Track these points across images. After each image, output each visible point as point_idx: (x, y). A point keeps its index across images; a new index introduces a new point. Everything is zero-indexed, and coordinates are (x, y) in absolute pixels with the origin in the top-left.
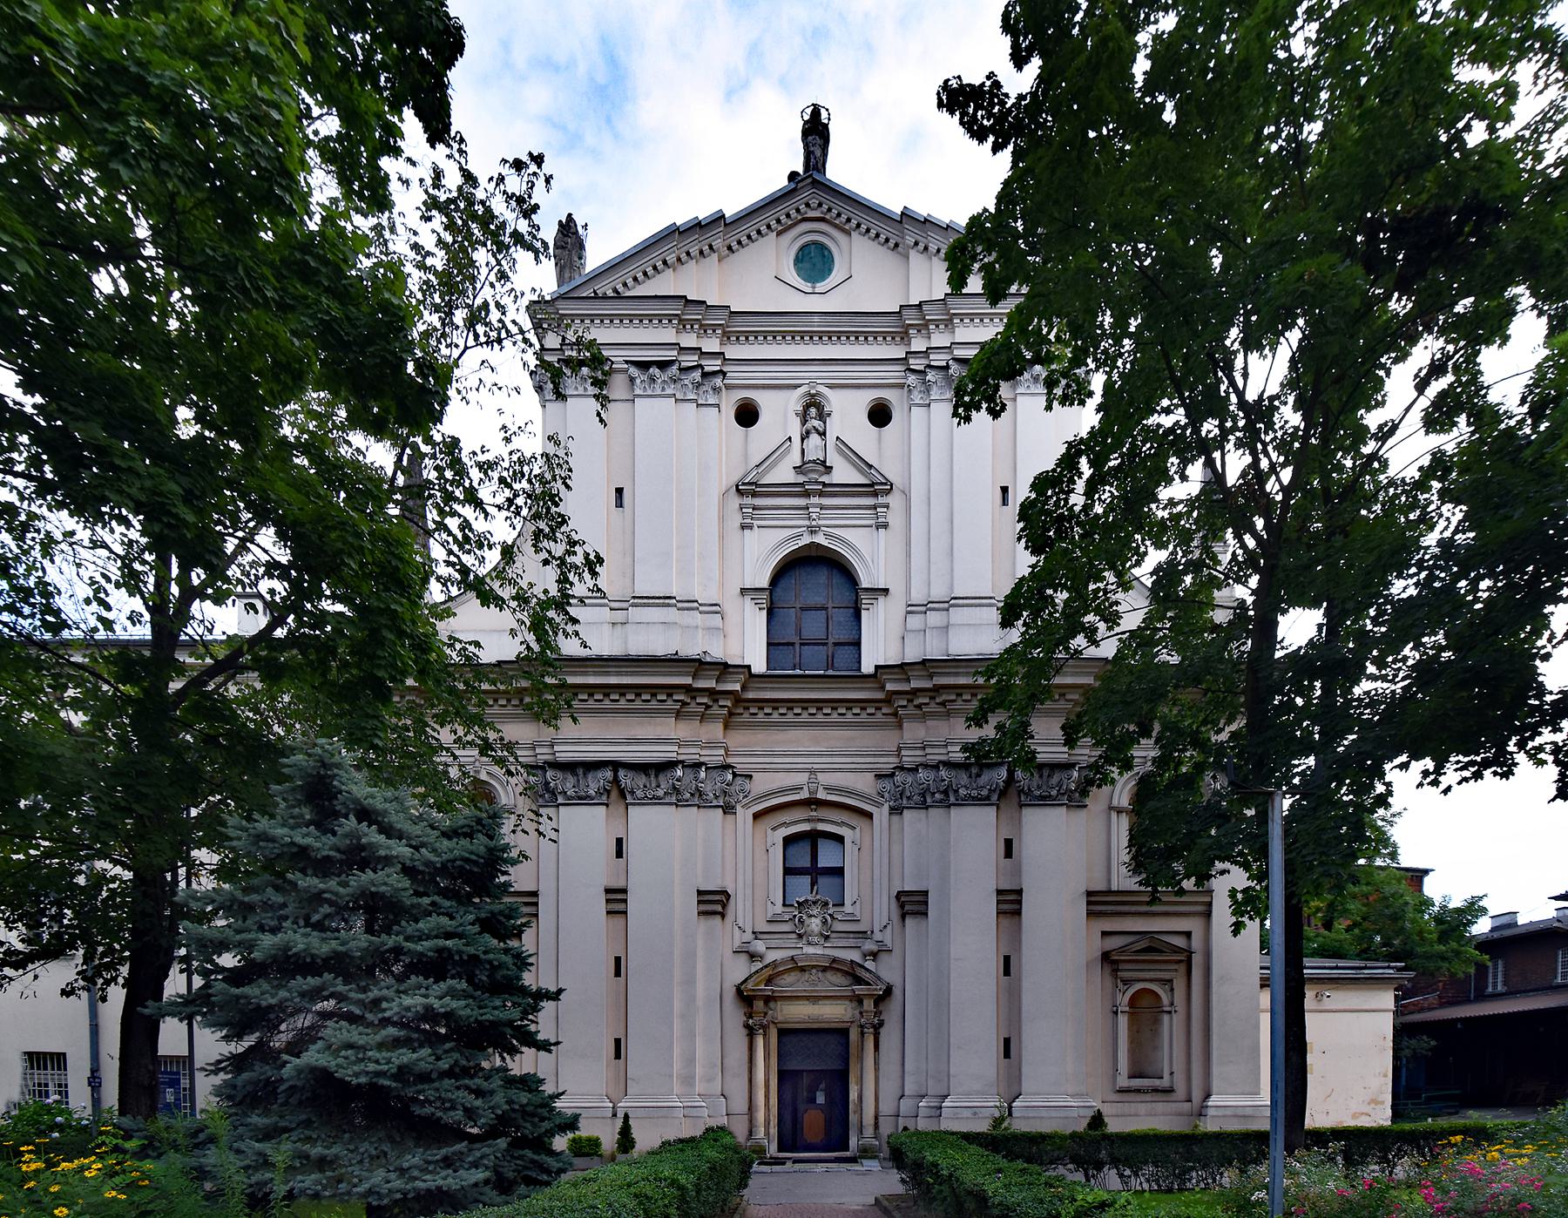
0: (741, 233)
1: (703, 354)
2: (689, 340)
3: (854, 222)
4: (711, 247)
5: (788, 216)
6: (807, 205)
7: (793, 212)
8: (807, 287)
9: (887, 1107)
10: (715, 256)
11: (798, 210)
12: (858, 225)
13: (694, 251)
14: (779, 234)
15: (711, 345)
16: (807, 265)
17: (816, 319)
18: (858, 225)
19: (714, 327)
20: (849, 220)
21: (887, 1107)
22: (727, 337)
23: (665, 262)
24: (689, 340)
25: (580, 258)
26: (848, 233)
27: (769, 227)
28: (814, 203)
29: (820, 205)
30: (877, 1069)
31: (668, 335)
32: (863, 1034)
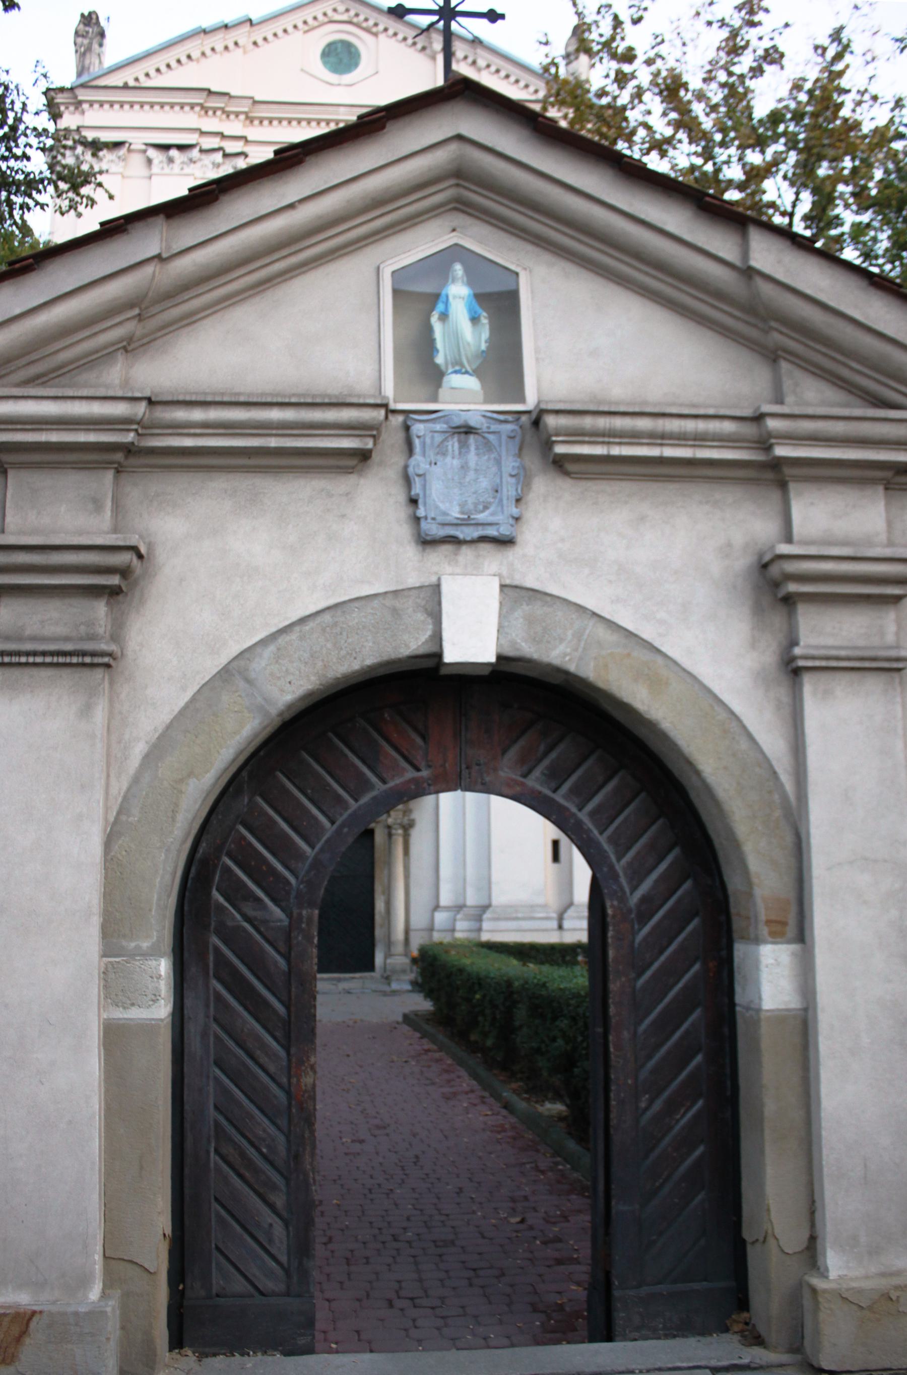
0: (267, 30)
1: (223, 136)
2: (211, 124)
3: (381, 27)
4: (236, 44)
5: (315, 18)
6: (335, 10)
7: (321, 18)
8: (333, 78)
9: (419, 920)
10: (239, 51)
11: (325, 14)
12: (386, 30)
13: (219, 47)
14: (306, 32)
15: (234, 127)
16: (332, 59)
17: (342, 109)
18: (386, 30)
19: (237, 114)
20: (376, 25)
21: (419, 920)
22: (250, 119)
23: (189, 57)
24: (211, 124)
25: (101, 45)
26: (376, 35)
27: (295, 27)
28: (341, 8)
29: (347, 10)
30: (407, 877)
31: (191, 119)
32: (390, 835)
